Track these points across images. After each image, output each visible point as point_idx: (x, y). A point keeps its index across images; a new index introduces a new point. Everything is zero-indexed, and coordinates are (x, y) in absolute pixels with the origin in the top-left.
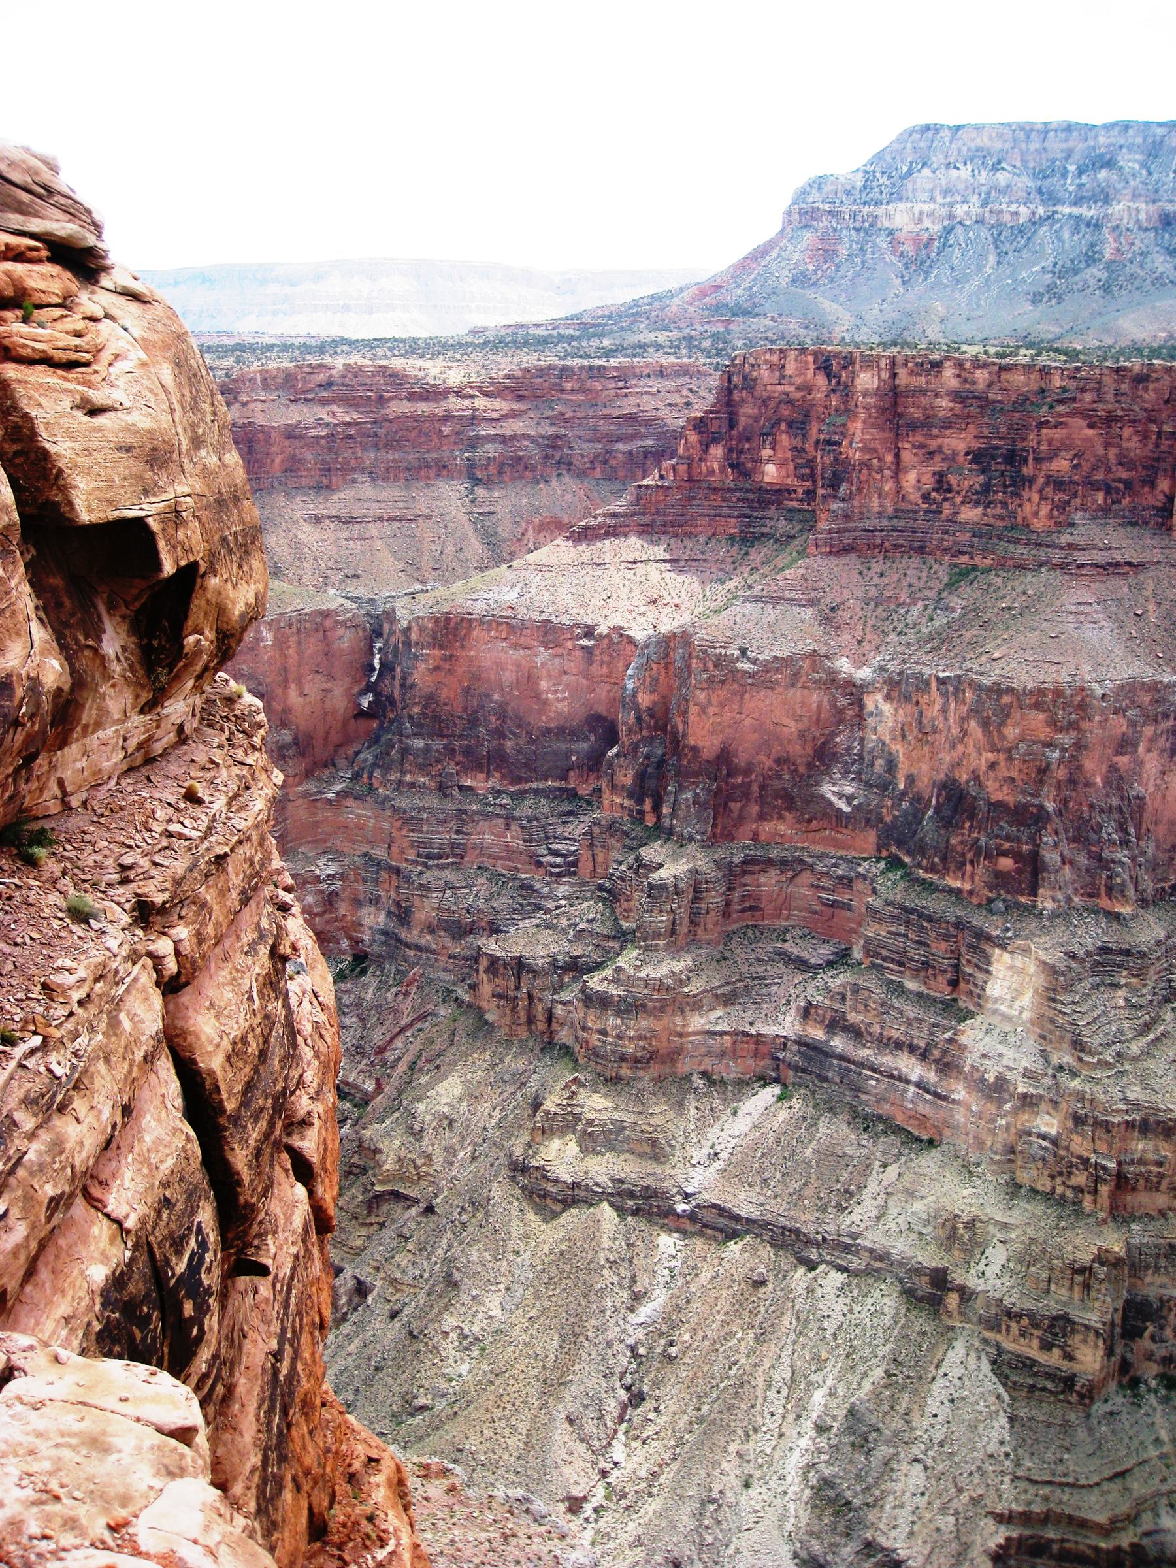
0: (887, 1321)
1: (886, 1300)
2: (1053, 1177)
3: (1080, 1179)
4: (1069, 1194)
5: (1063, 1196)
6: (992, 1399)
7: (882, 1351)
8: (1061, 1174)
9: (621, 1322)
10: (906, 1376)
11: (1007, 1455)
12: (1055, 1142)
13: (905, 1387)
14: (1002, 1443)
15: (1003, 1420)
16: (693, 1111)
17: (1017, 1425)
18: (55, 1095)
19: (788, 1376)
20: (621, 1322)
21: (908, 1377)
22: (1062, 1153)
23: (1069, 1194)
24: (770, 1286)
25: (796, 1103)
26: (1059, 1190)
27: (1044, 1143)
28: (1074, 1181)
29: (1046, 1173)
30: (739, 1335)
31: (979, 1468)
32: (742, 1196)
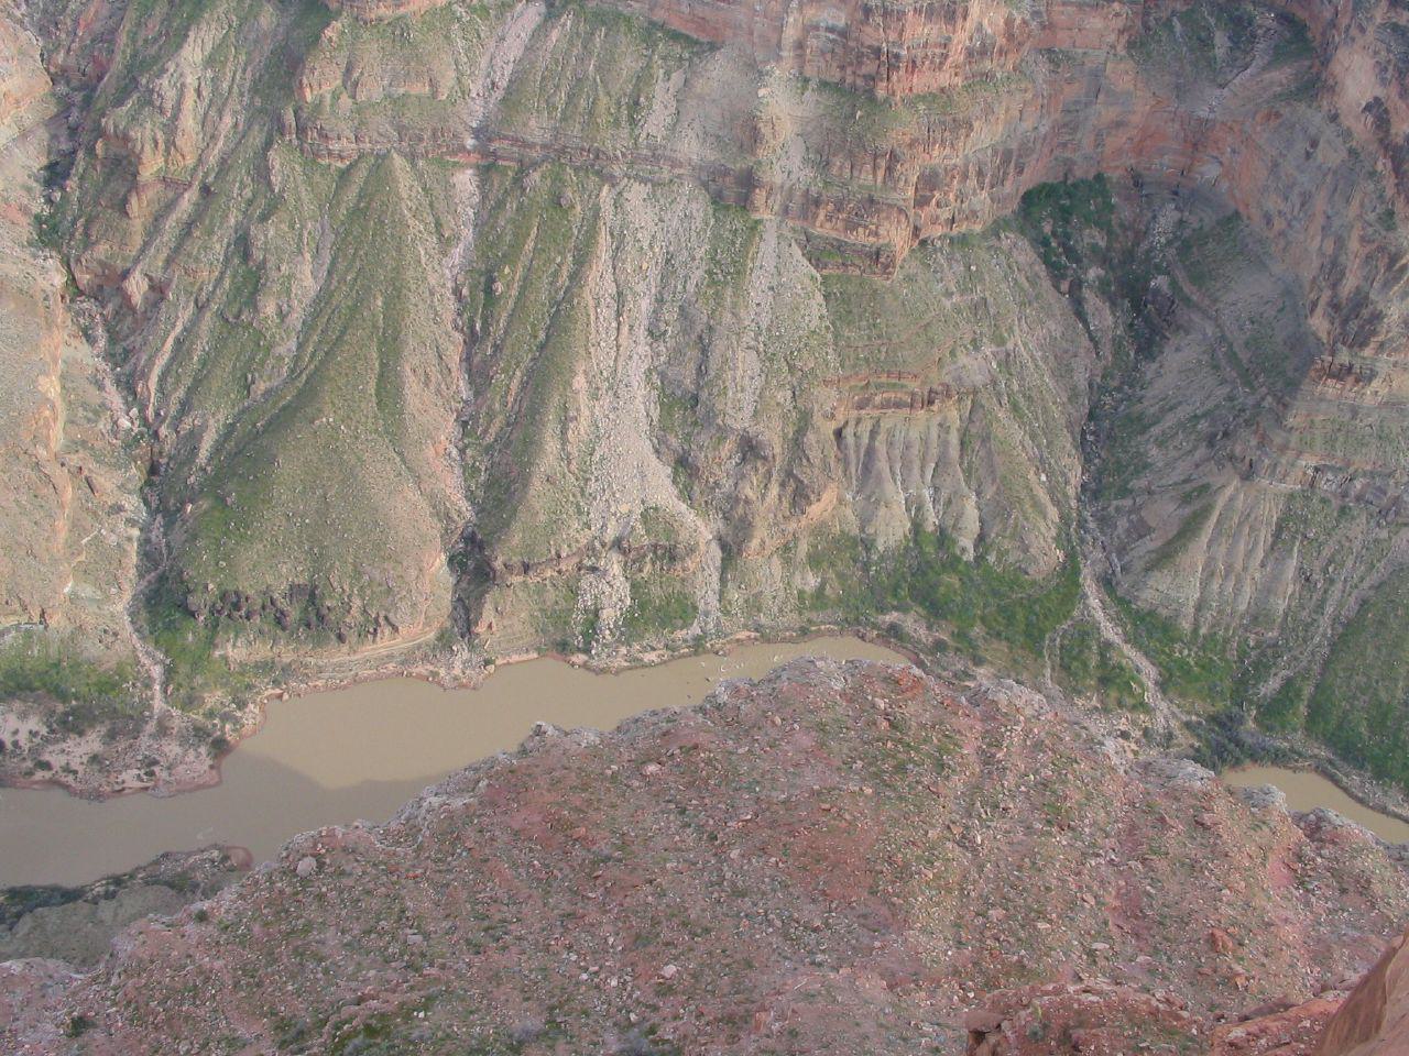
0: (699, 223)
1: (694, 205)
2: (842, 68)
3: (869, 67)
4: (860, 82)
5: (854, 86)
6: (807, 281)
7: (699, 253)
8: (851, 64)
9: (437, 267)
10: (728, 270)
11: (827, 328)
12: (844, 34)
13: (726, 283)
14: (821, 318)
15: (820, 298)
16: (460, 43)
17: (833, 303)
18: (250, 274)
19: (613, 290)
20: (437, 267)
21: (729, 273)
22: (852, 44)
23: (860, 82)
24: (579, 208)
25: (567, 20)
26: (849, 80)
27: (832, 36)
28: (864, 70)
29: (835, 65)
30: (559, 260)
31: (806, 345)
32: (533, 123)
